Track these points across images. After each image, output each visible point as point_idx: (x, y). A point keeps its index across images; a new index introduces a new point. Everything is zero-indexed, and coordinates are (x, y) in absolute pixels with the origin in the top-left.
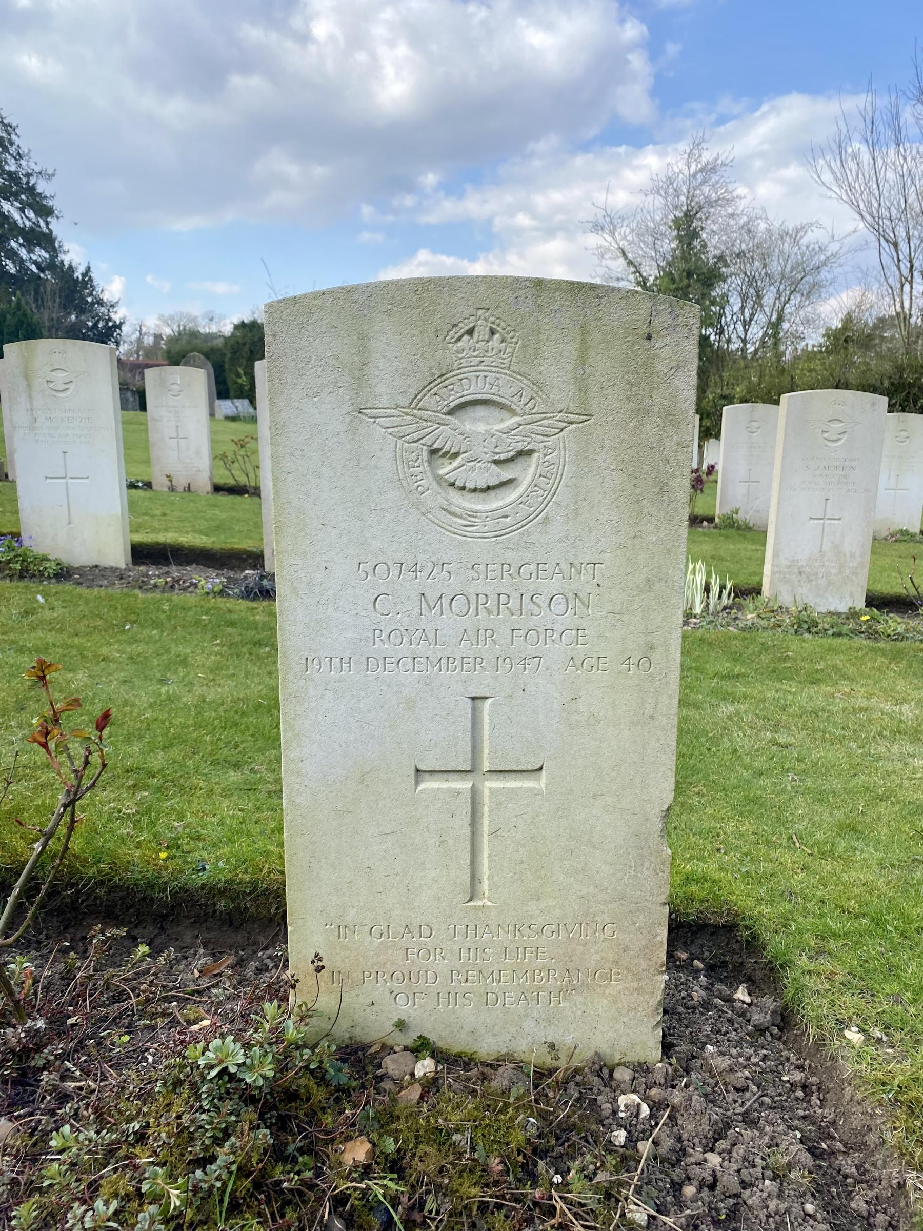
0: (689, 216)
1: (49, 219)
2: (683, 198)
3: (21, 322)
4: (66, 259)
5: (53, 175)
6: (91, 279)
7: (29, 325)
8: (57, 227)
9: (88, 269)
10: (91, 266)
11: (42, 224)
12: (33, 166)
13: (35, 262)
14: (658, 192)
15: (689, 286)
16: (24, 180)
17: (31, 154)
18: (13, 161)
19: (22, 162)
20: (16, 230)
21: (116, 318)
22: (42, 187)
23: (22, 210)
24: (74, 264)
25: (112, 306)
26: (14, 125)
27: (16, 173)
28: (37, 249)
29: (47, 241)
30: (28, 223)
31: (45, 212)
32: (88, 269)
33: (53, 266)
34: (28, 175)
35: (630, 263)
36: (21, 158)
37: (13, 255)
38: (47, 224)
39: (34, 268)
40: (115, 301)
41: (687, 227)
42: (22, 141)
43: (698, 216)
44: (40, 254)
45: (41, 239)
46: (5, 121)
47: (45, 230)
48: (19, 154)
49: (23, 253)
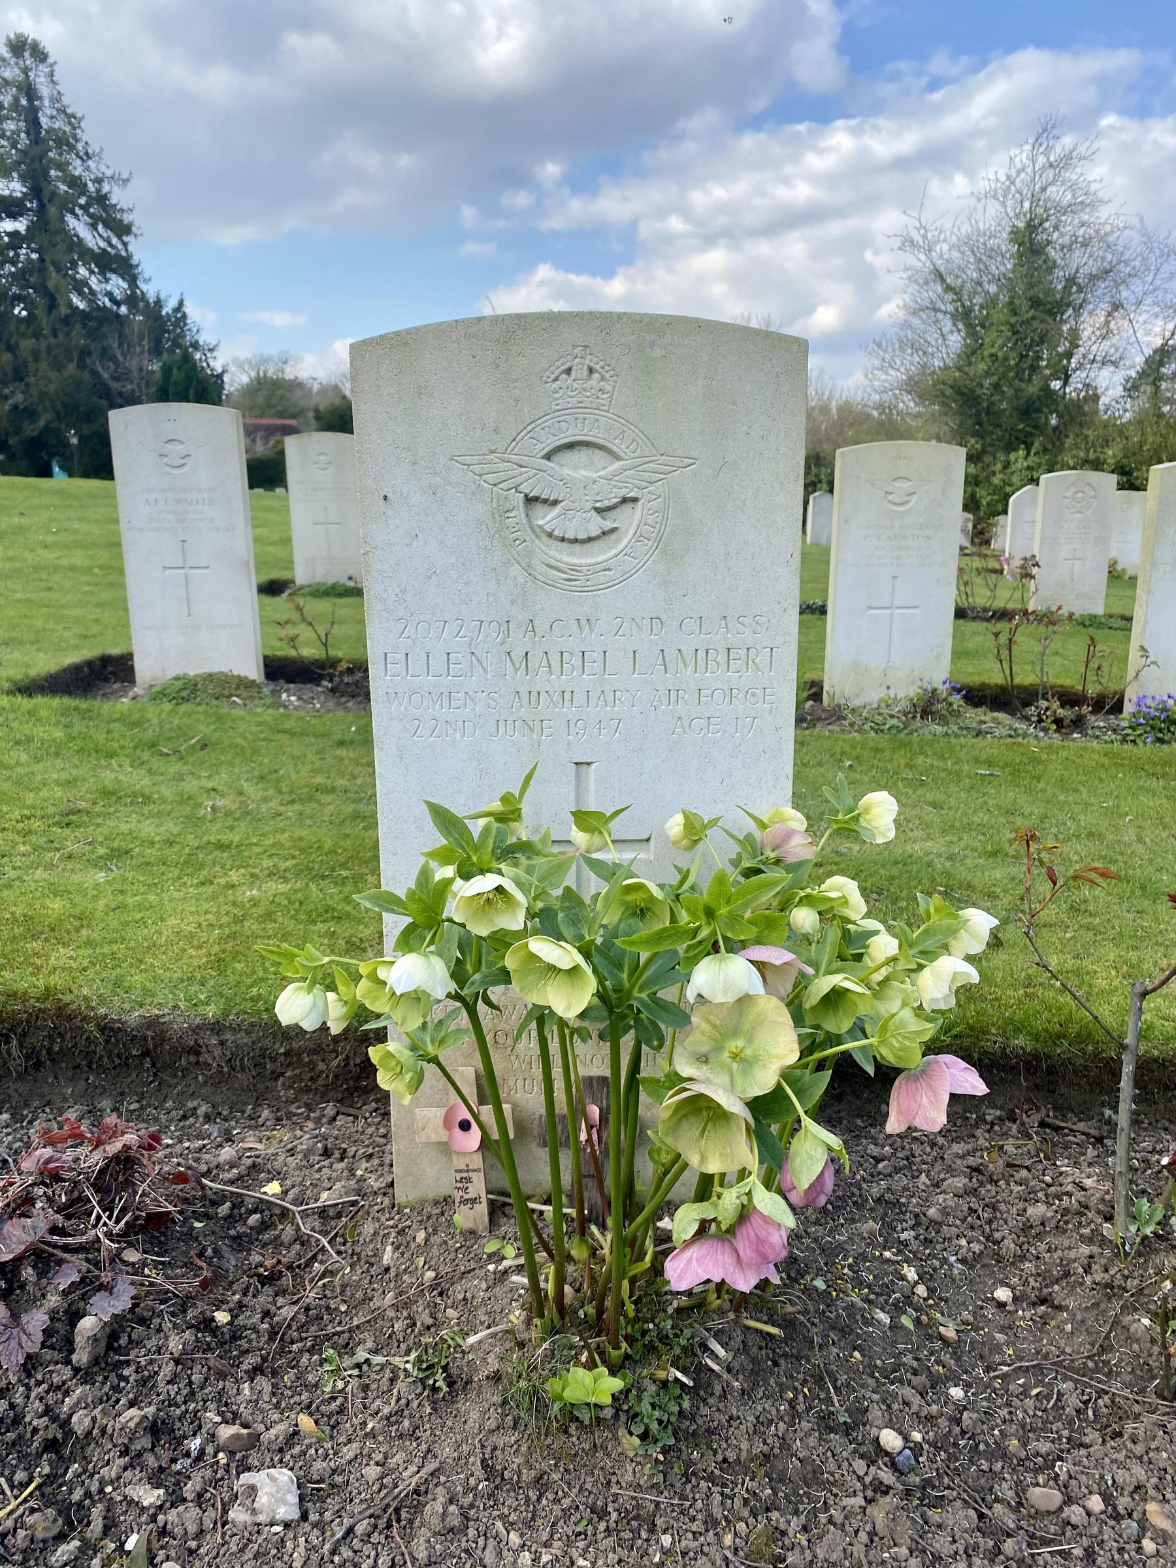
0: (1032, 227)
1: (125, 239)
2: (1027, 205)
3: (189, 378)
4: (150, 290)
5: (128, 180)
6: (184, 316)
7: (200, 382)
8: (138, 250)
9: (181, 303)
10: (185, 298)
11: (120, 246)
12: (103, 168)
13: (110, 295)
14: (995, 197)
15: (1033, 318)
16: (91, 187)
17: (104, 156)
18: (79, 162)
19: (90, 163)
20: (87, 255)
21: (217, 365)
22: (118, 196)
23: (94, 227)
24: (163, 296)
25: (211, 350)
26: (79, 115)
27: (80, 177)
28: (113, 277)
29: (125, 267)
30: (102, 244)
31: (123, 230)
32: (181, 303)
33: (134, 299)
34: (98, 181)
35: (949, 289)
36: (89, 157)
37: (80, 286)
38: (125, 244)
39: (107, 300)
40: (214, 343)
41: (1030, 242)
42: (90, 135)
43: (1047, 225)
44: (117, 285)
45: (116, 263)
46: (69, 111)
47: (124, 253)
48: (87, 153)
49: (94, 282)
